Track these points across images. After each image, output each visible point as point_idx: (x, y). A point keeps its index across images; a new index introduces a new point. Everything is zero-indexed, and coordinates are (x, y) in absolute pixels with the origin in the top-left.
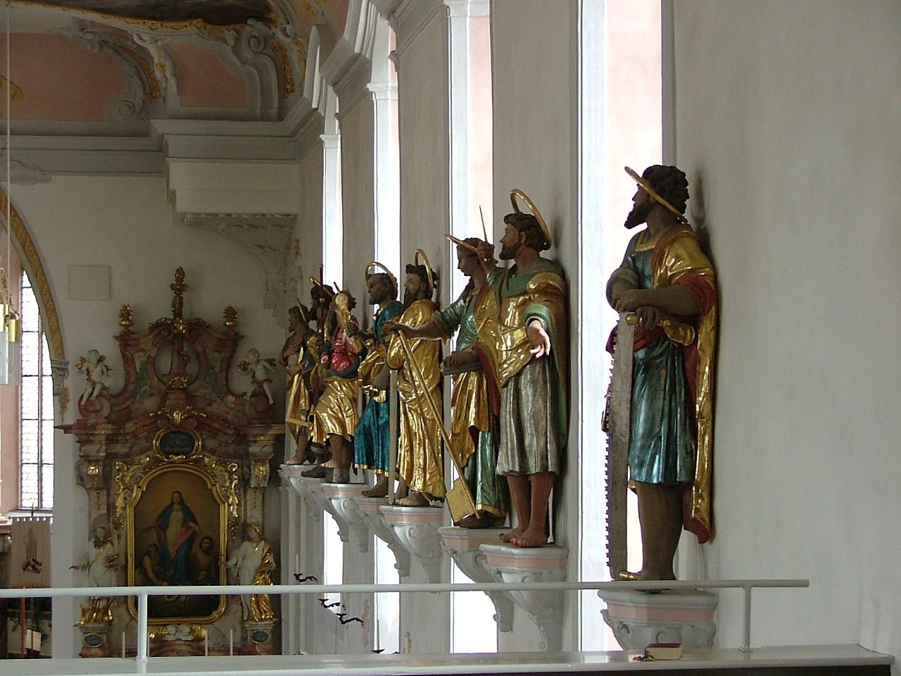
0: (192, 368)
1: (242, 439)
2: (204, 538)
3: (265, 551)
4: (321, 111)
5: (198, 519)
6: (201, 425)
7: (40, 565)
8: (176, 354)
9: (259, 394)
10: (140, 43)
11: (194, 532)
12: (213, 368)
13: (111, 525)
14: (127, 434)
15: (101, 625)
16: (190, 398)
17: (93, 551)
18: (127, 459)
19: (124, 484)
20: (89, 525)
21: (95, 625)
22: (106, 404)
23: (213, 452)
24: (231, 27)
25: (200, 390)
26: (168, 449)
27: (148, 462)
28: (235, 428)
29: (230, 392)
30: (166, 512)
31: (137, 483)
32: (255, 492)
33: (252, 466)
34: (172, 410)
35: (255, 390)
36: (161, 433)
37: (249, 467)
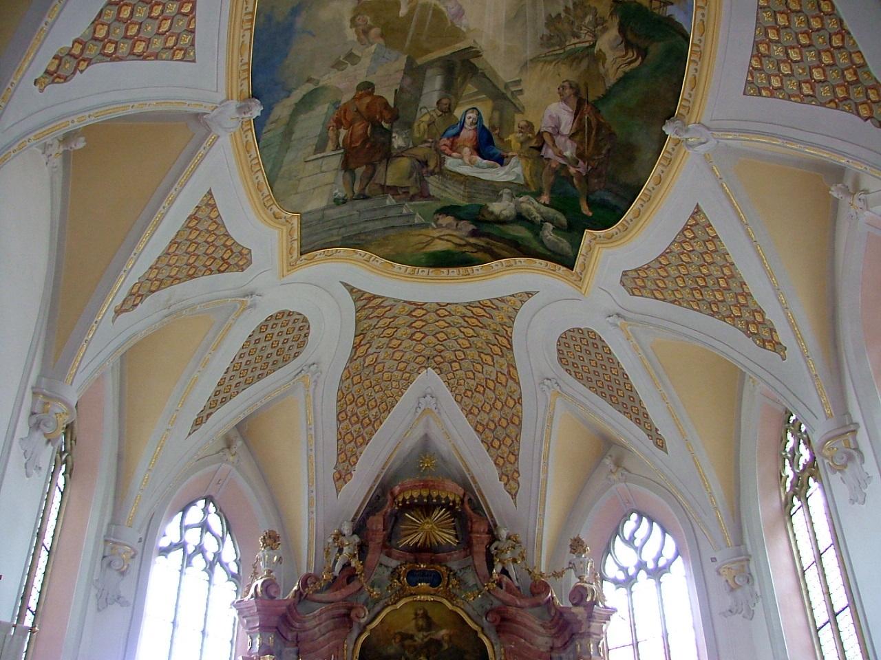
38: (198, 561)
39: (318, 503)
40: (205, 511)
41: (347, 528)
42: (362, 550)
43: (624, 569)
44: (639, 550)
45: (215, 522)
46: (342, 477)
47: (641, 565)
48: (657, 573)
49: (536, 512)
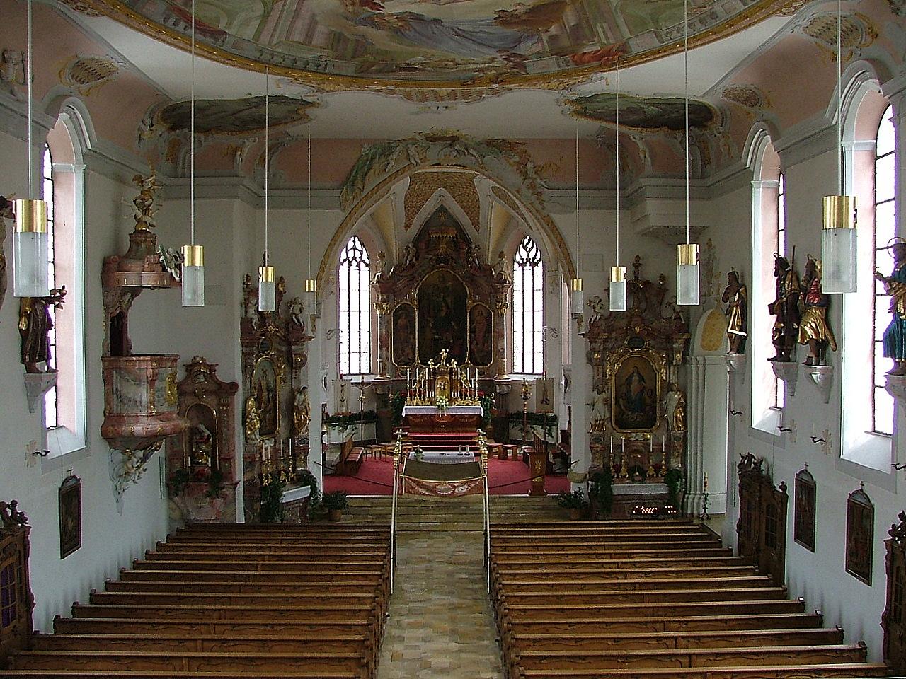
0: (643, 305)
1: (669, 340)
4: (752, 169)
5: (646, 381)
10: (634, 140)
11: (644, 387)
12: (654, 305)
17: (597, 397)
18: (612, 351)
21: (598, 433)
25: (647, 316)
28: (666, 336)
29: (662, 318)
30: (631, 377)
37: (673, 354)
38: (354, 263)
39: (399, 235)
40: (354, 241)
42: (417, 255)
43: (523, 259)
45: (358, 245)
46: (407, 227)
47: (528, 260)
48: (534, 265)
49: (489, 236)
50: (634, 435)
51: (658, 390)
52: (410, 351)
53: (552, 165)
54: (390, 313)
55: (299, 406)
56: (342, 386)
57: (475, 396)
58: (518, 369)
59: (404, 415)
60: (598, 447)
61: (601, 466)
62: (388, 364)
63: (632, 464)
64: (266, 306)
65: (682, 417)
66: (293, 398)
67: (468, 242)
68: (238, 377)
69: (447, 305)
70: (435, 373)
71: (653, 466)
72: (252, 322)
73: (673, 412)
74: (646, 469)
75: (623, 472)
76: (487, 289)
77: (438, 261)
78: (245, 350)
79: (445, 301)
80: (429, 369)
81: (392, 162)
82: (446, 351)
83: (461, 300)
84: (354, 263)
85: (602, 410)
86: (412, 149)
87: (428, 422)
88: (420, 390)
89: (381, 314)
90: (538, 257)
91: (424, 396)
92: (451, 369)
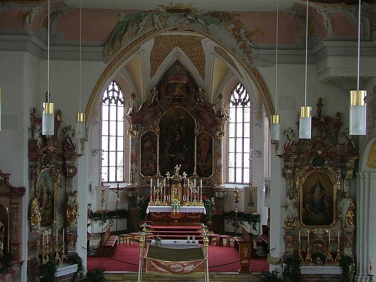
0: (324, 135)
1: (343, 160)
2: (327, 197)
3: (351, 202)
5: (326, 190)
6: (328, 156)
7: (254, 204)
8: (319, 129)
9: (350, 144)
10: (320, 13)
12: (332, 135)
13: (294, 191)
14: (301, 158)
15: (292, 228)
16: (324, 145)
17: (289, 201)
18: (301, 168)
19: (299, 176)
20: (286, 191)
21: (289, 228)
22: (294, 147)
23: (331, 165)
24: (355, 5)
25: (327, 142)
26: (316, 164)
27: (308, 169)
30: (314, 187)
31: (304, 176)
32: (347, 180)
33: (347, 171)
34: (318, 149)
35: (348, 143)
36: (313, 158)
38: (113, 101)
39: (146, 81)
40: (113, 85)
41: (154, 89)
42: (159, 96)
43: (236, 100)
44: (240, 95)
46: (152, 75)
47: (240, 100)
48: (244, 104)
49: (212, 82)
50: (316, 230)
51: (335, 197)
52: (153, 166)
53: (259, 31)
54: (139, 138)
55: (71, 205)
56: (103, 191)
57: (200, 199)
58: (231, 180)
59: (148, 212)
60: (290, 238)
61: (292, 253)
62: (137, 175)
63: (315, 251)
64: (48, 132)
65: (353, 217)
66: (66, 199)
67: (196, 87)
68: (26, 183)
69: (180, 133)
70: (171, 182)
71: (331, 253)
72: (37, 143)
73: (345, 212)
74: (325, 255)
75: (308, 257)
76: (210, 121)
77: (175, 100)
78: (31, 163)
79: (179, 130)
80: (167, 179)
81: (142, 28)
82: (179, 166)
83: (190, 128)
84: (113, 101)
85: (293, 211)
86: (156, 18)
87: (165, 218)
88: (159, 195)
89: (132, 138)
90: (247, 98)
91: (163, 198)
92: (183, 179)
